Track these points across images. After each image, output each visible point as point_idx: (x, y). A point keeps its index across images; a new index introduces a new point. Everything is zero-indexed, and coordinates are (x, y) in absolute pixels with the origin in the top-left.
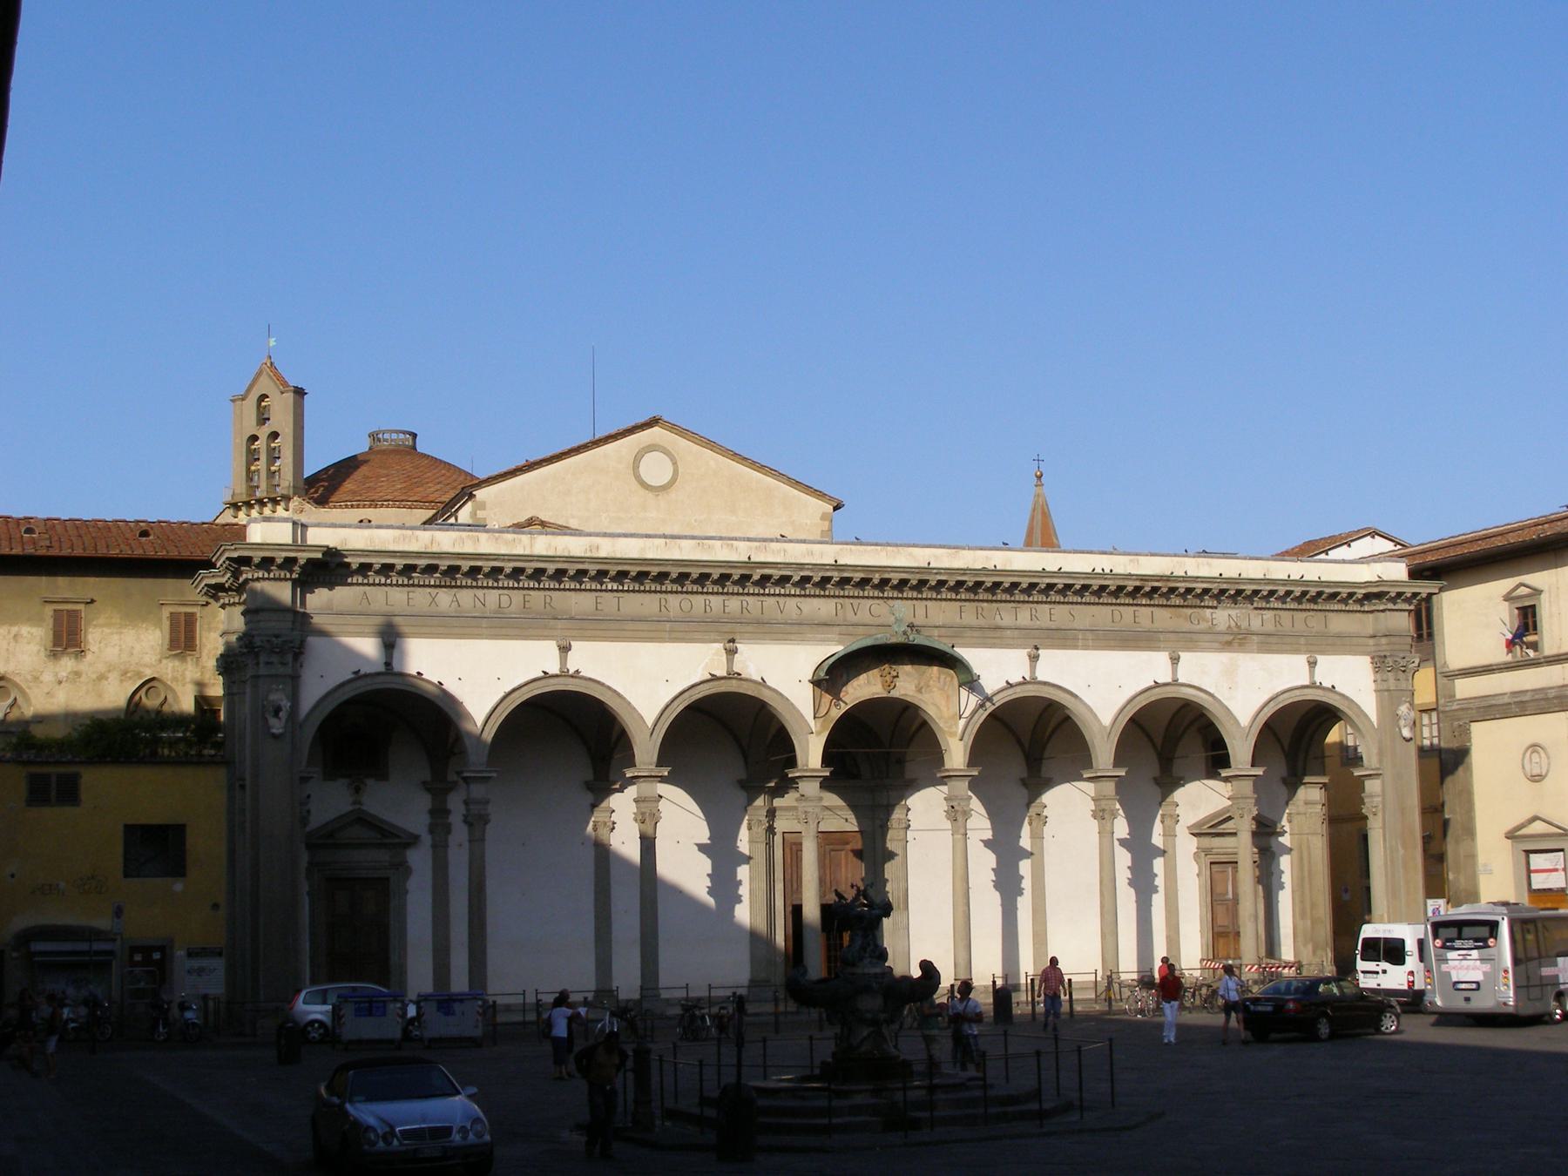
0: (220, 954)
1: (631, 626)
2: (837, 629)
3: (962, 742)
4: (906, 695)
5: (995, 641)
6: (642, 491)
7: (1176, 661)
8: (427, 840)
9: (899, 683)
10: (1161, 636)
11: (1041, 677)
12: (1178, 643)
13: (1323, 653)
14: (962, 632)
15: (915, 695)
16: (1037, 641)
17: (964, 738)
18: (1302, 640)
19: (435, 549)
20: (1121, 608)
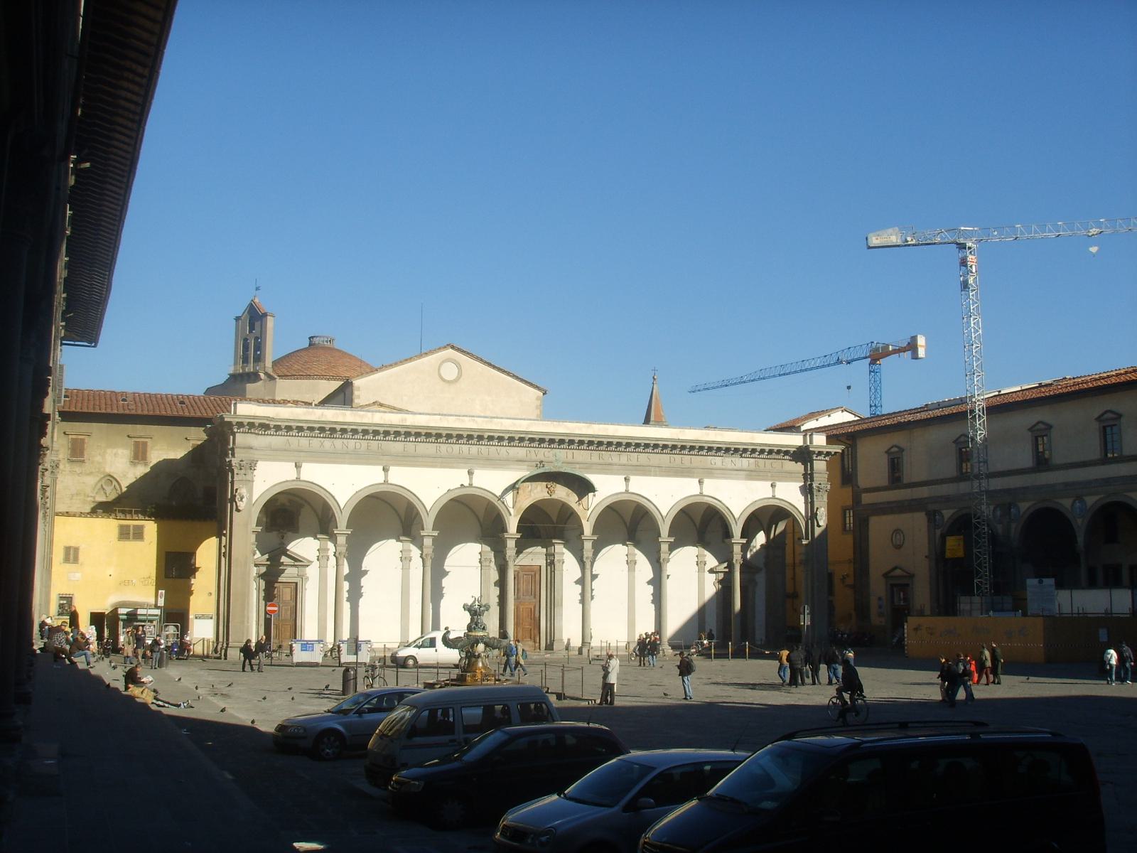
0: (211, 618)
1: (421, 459)
2: (526, 463)
3: (589, 522)
6: (442, 383)
8: (316, 564)
11: (631, 490)
12: (702, 475)
13: (780, 481)
14: (590, 467)
16: (628, 472)
18: (769, 475)
19: (323, 419)
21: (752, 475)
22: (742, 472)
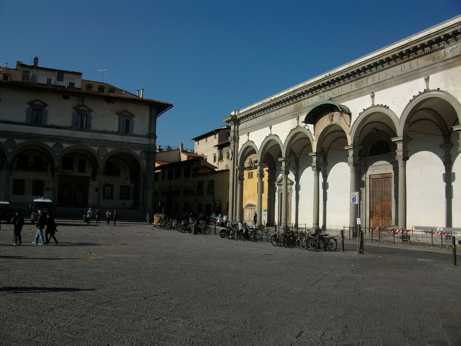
4: (336, 122)
7: (427, 80)
9: (334, 118)
10: (421, 71)
14: (349, 96)
15: (338, 121)
20: (404, 64)
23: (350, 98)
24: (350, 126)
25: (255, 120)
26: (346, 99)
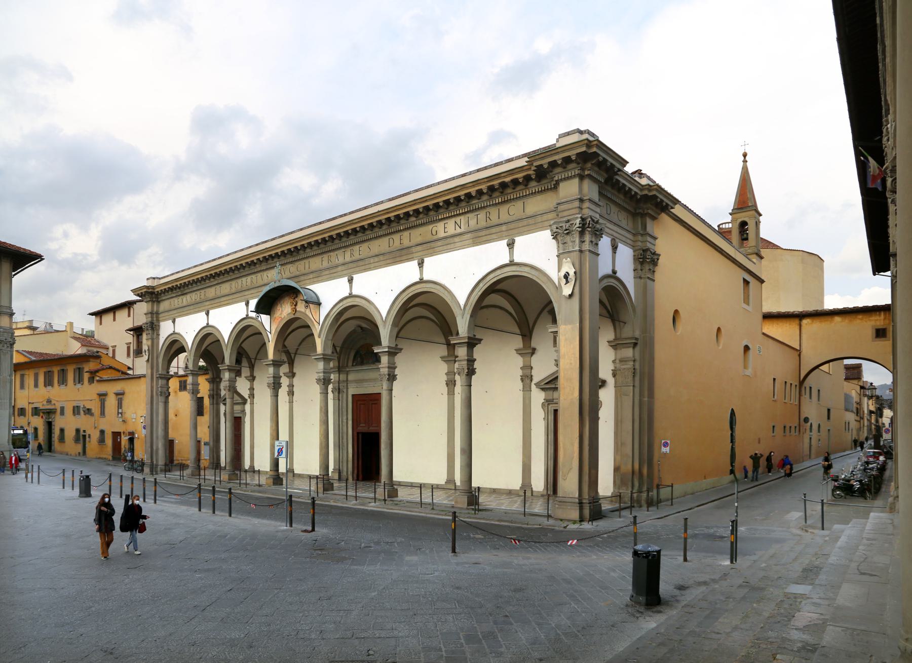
5: (335, 274)
8: (249, 400)
10: (414, 249)
14: (320, 275)
17: (322, 336)
18: (504, 228)
21: (479, 237)
22: (469, 235)
23: (320, 278)
24: (319, 324)
25: (184, 298)
26: (315, 280)
